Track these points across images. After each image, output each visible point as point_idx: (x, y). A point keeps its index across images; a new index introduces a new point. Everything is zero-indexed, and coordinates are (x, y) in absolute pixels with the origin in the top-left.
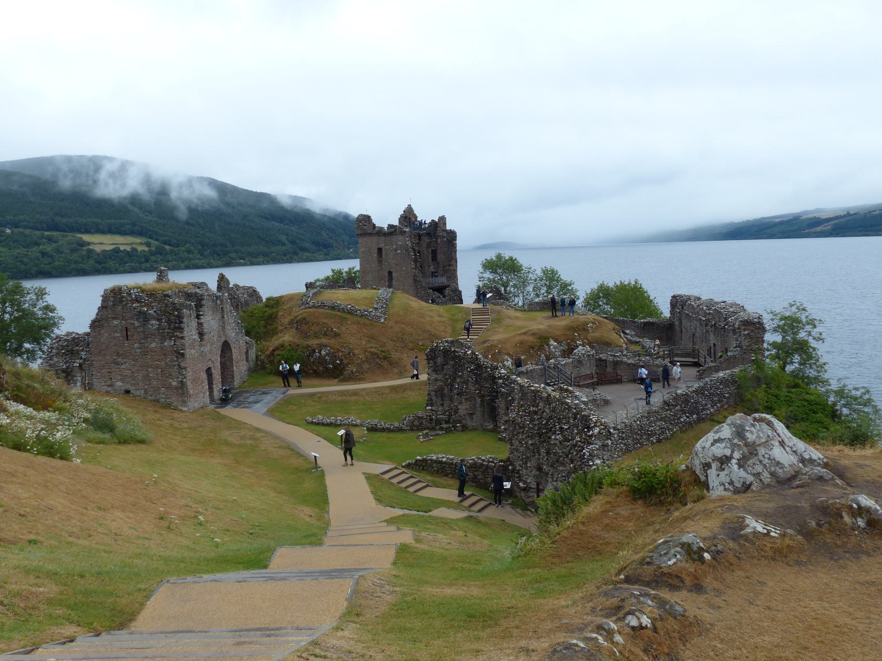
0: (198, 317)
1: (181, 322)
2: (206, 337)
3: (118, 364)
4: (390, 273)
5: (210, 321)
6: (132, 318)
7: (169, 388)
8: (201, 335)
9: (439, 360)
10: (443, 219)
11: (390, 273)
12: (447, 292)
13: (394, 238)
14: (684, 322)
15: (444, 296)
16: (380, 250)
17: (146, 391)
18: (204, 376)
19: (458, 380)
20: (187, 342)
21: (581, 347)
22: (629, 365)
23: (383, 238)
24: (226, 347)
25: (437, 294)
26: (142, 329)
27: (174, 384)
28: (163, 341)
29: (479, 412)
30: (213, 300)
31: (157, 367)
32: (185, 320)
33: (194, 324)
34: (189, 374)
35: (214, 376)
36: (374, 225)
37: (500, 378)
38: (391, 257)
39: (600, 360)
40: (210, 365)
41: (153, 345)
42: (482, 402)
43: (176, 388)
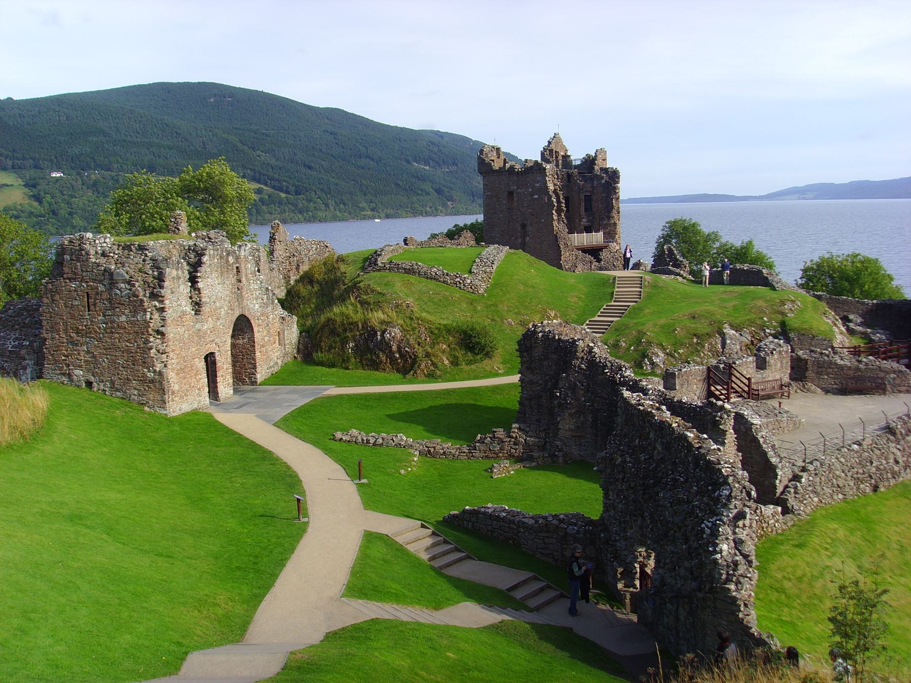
0: (193, 280)
2: (205, 309)
3: (77, 345)
4: (524, 226)
5: (213, 284)
6: (94, 280)
7: (144, 380)
8: (197, 306)
10: (602, 151)
11: (524, 226)
12: (604, 254)
15: (599, 261)
16: (511, 194)
17: (112, 383)
18: (201, 365)
19: (561, 384)
20: (170, 314)
21: (771, 338)
22: (841, 368)
23: (515, 178)
24: (242, 326)
25: (589, 257)
26: (105, 296)
27: (150, 375)
28: (135, 313)
30: (221, 257)
31: (128, 351)
32: (166, 284)
33: (185, 288)
34: (173, 361)
35: (218, 365)
38: (526, 204)
39: (799, 359)
40: (212, 348)
43: (152, 381)
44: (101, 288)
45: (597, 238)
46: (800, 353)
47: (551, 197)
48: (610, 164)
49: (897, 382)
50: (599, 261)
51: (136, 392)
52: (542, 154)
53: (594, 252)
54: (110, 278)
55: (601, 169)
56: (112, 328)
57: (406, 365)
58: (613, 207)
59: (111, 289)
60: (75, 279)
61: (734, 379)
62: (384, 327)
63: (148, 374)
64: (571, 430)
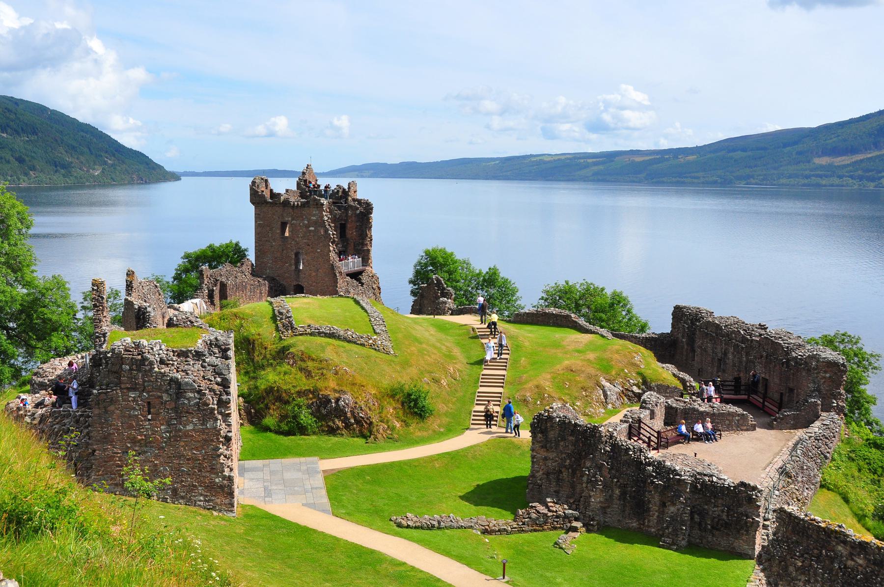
1: (228, 394)
4: (297, 255)
6: (159, 389)
9: (552, 435)
11: (297, 255)
12: (364, 278)
13: (306, 211)
14: (698, 342)
15: (362, 284)
22: (702, 413)
26: (173, 405)
29: (616, 505)
31: (194, 459)
36: (271, 190)
37: (649, 464)
38: (301, 235)
41: (190, 427)
42: (623, 494)
43: (222, 487)
44: (165, 397)
45: (353, 263)
46: (669, 401)
47: (328, 230)
48: (359, 196)
49: (741, 422)
50: (362, 284)
51: (202, 498)
52: (298, 184)
53: (356, 276)
54: (178, 388)
55: (354, 200)
56: (176, 437)
57: (362, 429)
58: (367, 235)
59: (178, 398)
60: (133, 389)
61: (642, 431)
62: (337, 395)
63: (217, 480)
64: (600, 502)
